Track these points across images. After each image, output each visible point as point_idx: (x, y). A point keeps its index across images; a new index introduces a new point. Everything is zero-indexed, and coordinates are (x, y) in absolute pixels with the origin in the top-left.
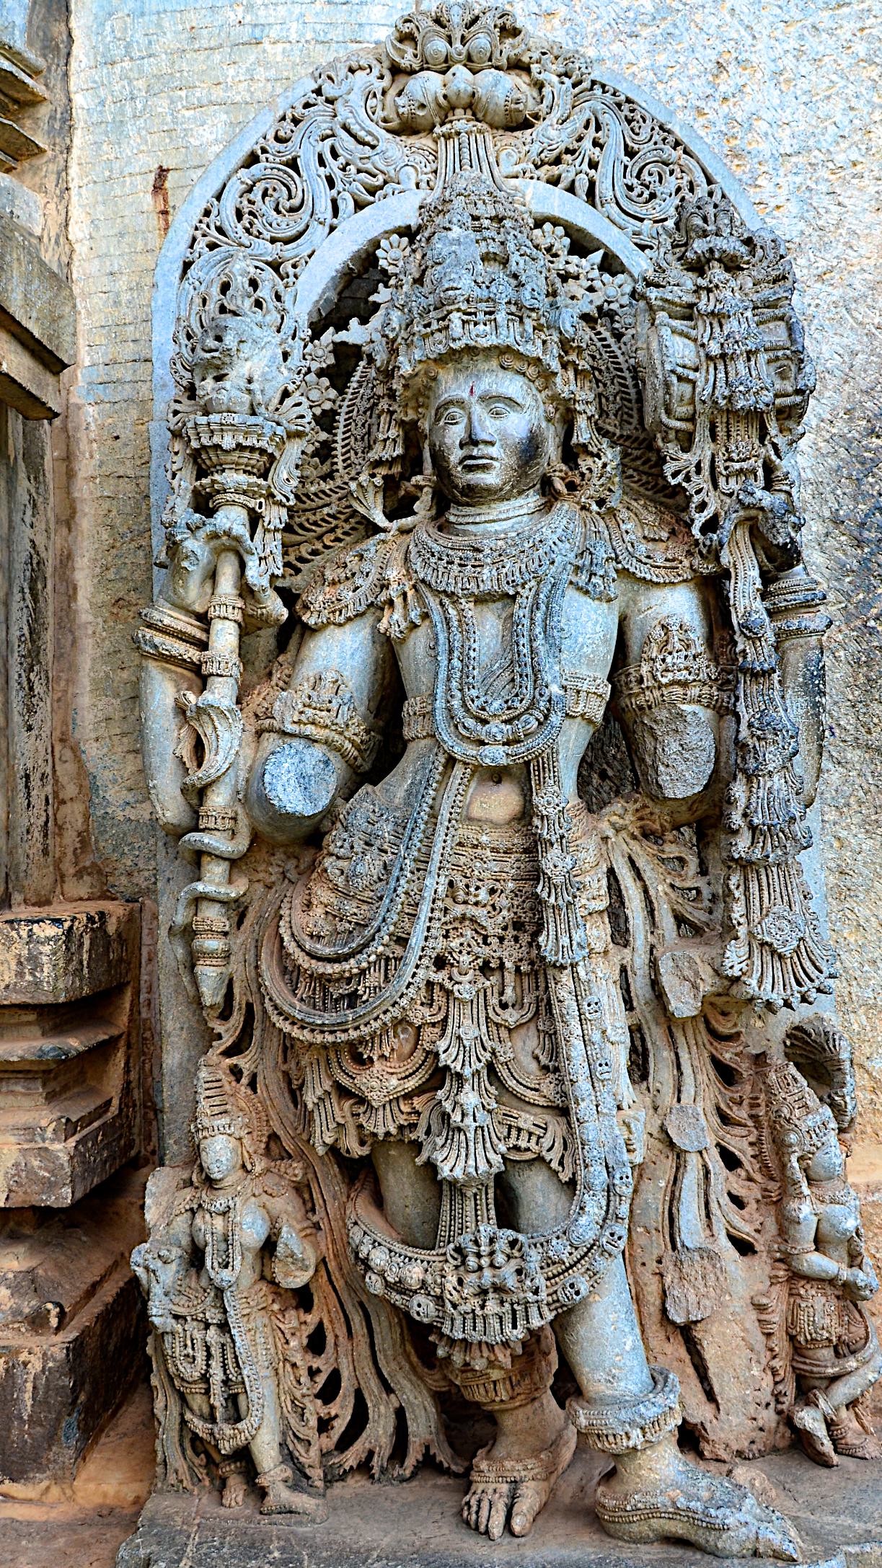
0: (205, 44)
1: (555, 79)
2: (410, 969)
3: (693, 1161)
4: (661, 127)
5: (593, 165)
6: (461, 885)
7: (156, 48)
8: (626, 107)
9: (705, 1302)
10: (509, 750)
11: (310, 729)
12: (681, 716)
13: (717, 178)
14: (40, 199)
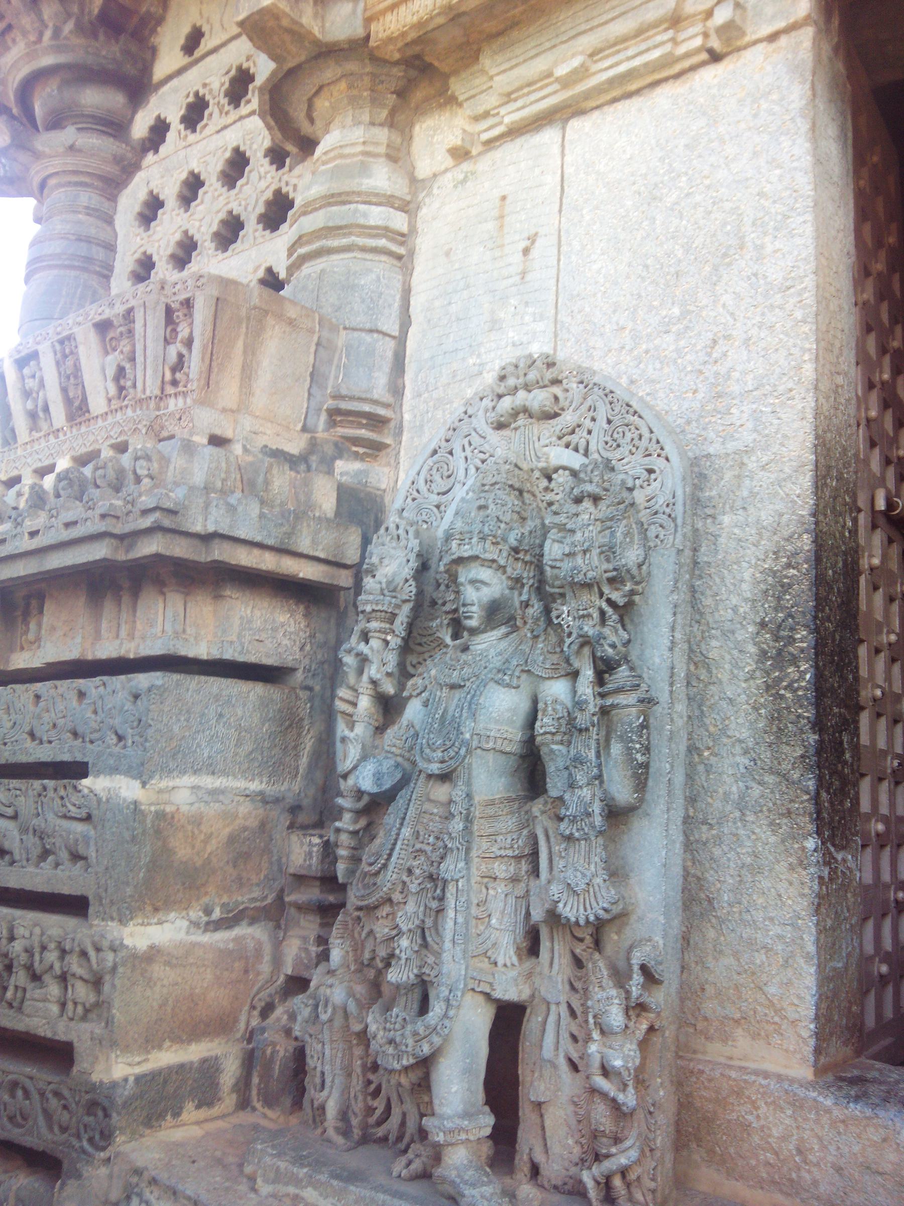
0: (459, 378)
1: (575, 385)
2: (390, 873)
3: (553, 1008)
4: (628, 405)
5: (590, 432)
6: (421, 833)
7: (439, 384)
8: (610, 396)
9: (548, 1093)
10: (439, 765)
11: (394, 749)
12: (552, 751)
13: (654, 430)
14: (386, 470)
